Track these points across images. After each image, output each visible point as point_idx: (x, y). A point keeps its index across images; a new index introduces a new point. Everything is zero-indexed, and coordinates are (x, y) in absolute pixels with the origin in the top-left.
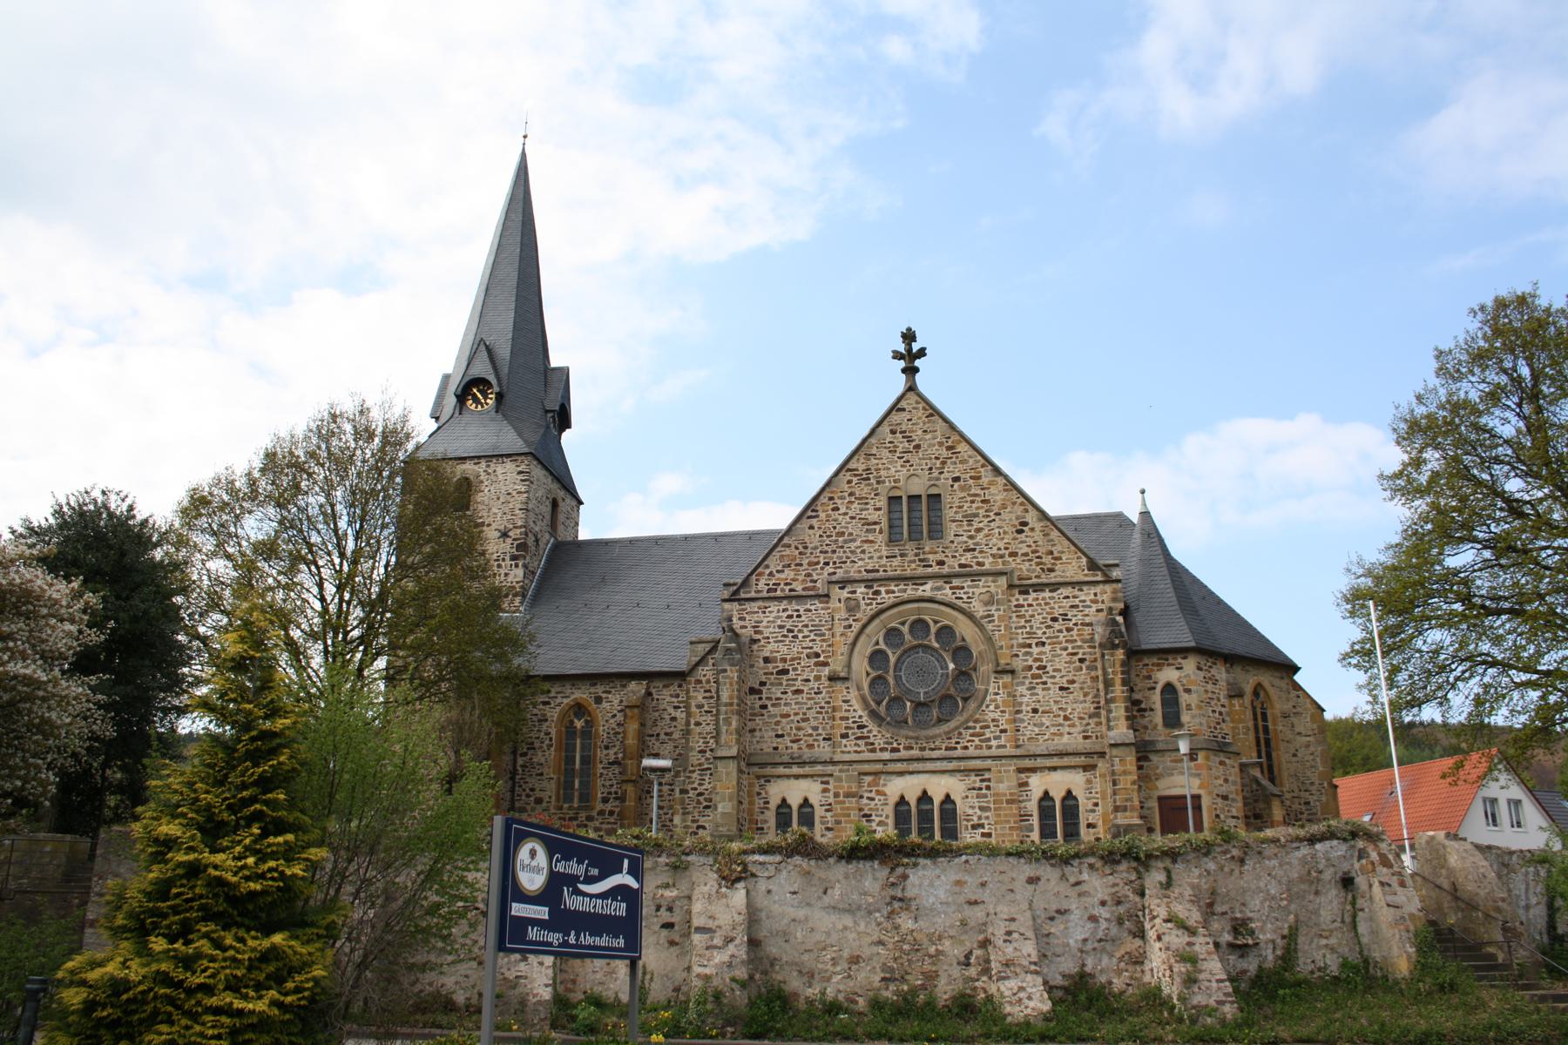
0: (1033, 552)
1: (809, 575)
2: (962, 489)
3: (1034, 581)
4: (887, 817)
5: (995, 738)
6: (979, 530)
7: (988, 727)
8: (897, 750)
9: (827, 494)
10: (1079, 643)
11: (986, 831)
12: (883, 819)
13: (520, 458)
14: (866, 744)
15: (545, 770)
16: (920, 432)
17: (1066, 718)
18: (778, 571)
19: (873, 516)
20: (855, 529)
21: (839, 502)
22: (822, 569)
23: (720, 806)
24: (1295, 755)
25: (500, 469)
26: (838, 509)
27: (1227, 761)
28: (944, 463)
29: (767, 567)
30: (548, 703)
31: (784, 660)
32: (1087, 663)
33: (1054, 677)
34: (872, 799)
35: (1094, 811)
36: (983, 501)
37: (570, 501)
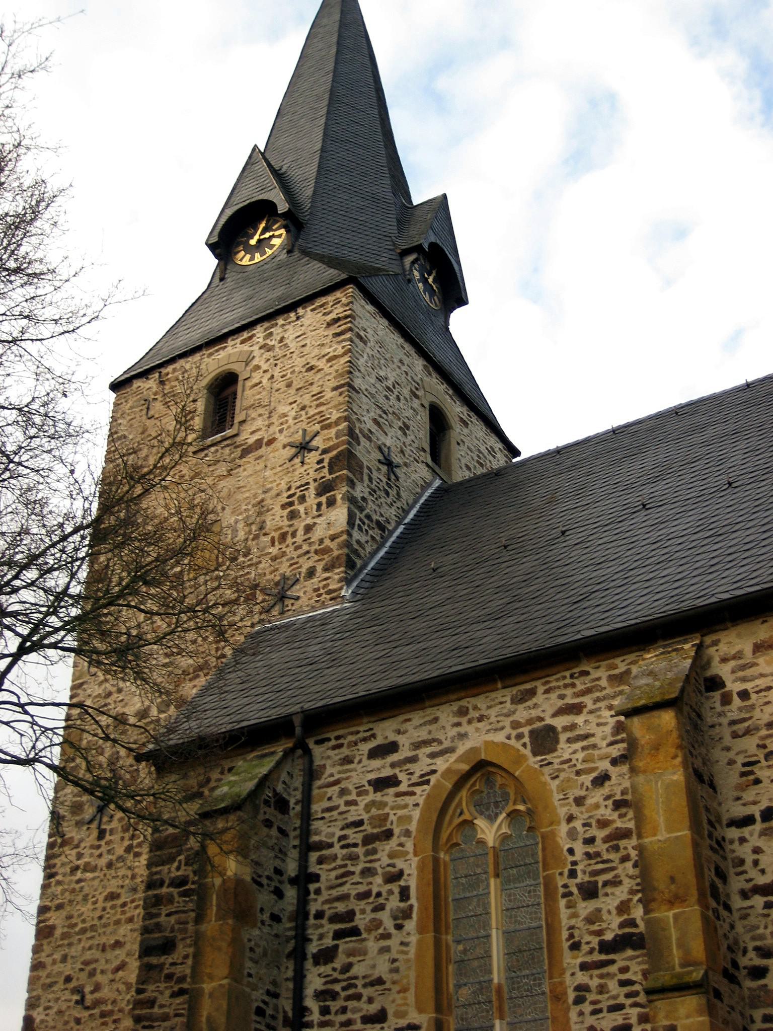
13: (330, 299)
15: (391, 1002)
25: (291, 334)
30: (390, 782)
37: (478, 429)
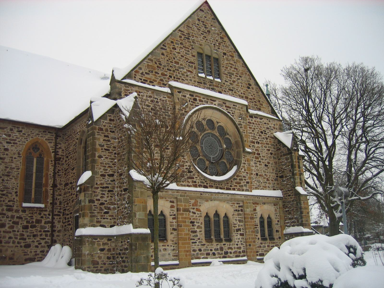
0: (254, 99)
1: (162, 80)
2: (227, 59)
4: (201, 223)
5: (245, 185)
6: (234, 82)
7: (242, 180)
10: (270, 146)
11: (242, 232)
12: (199, 224)
14: (193, 182)
16: (209, 25)
17: (268, 180)
18: (146, 73)
19: (192, 59)
21: (176, 46)
22: (169, 79)
23: (138, 214)
26: (175, 49)
28: (219, 44)
29: (141, 69)
32: (273, 155)
33: (263, 159)
34: (195, 213)
35: (277, 224)
36: (235, 68)
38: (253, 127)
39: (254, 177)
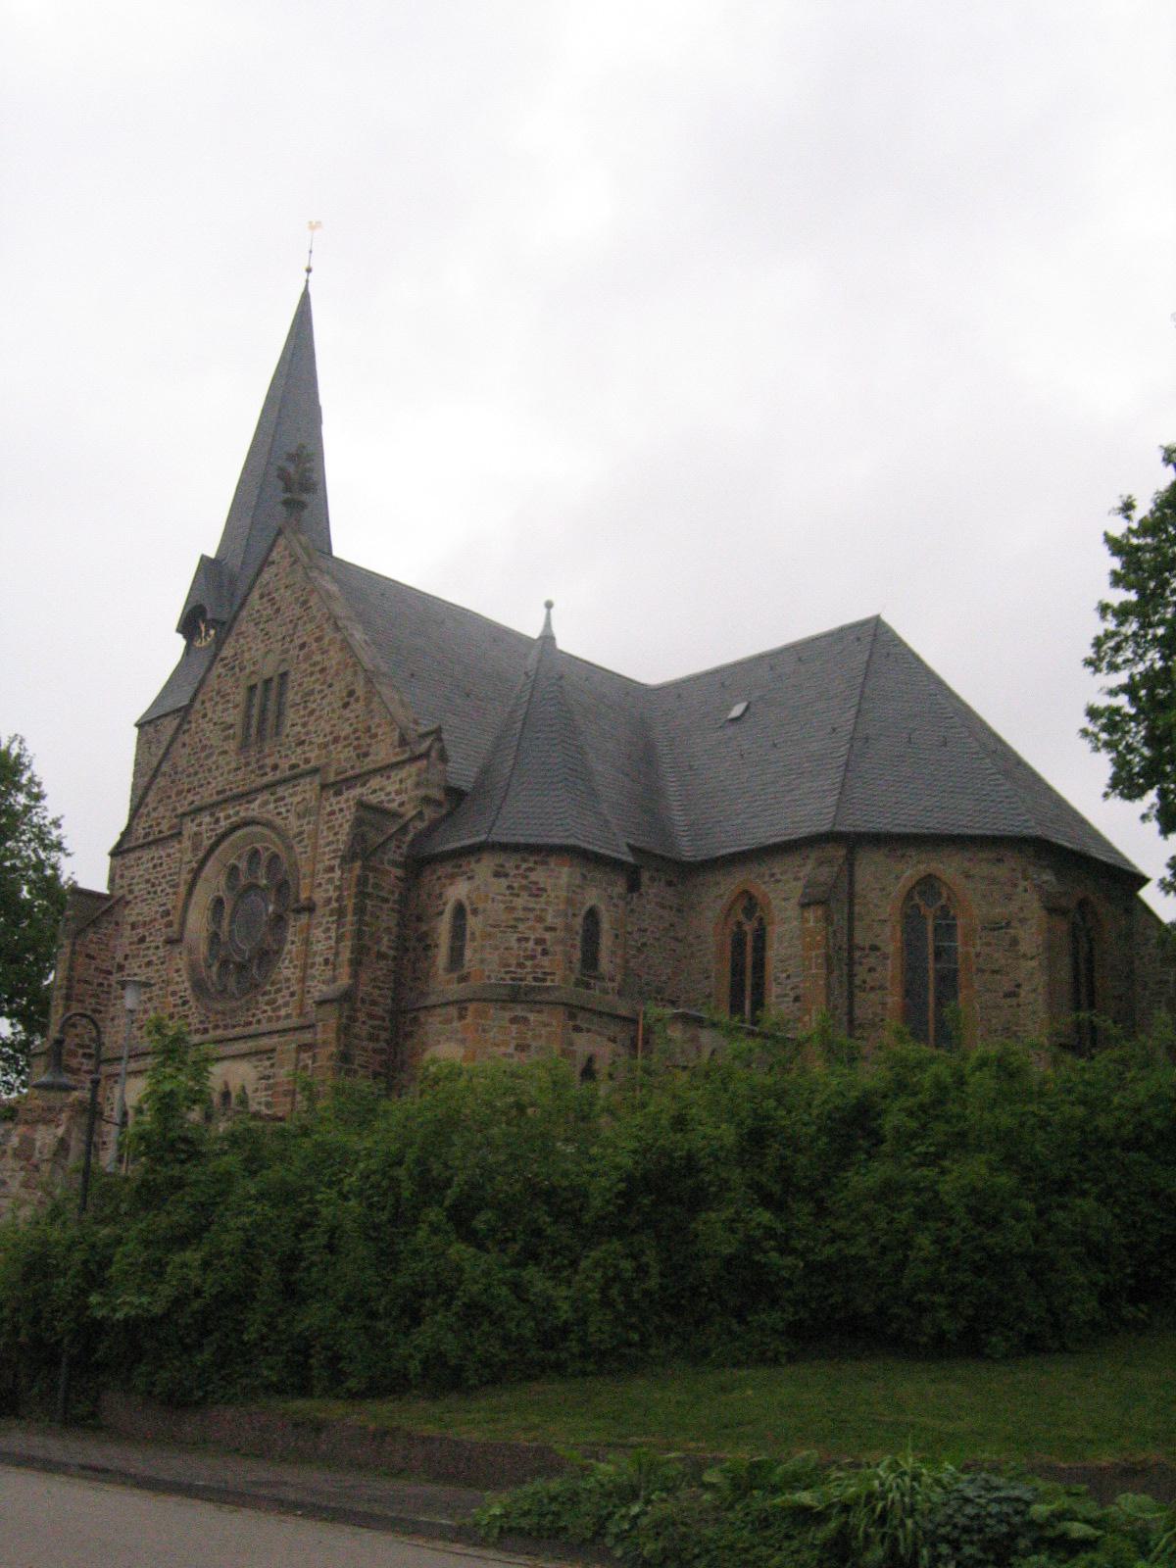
3: (350, 773)
6: (312, 712)
8: (206, 1031)
9: (200, 697)
18: (155, 809)
20: (214, 738)
24: (1008, 995)
27: (532, 1017)
28: (296, 625)
31: (145, 924)
38: (339, 822)
39: (317, 973)
